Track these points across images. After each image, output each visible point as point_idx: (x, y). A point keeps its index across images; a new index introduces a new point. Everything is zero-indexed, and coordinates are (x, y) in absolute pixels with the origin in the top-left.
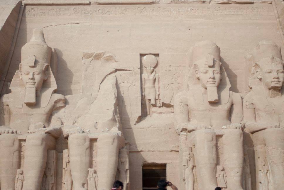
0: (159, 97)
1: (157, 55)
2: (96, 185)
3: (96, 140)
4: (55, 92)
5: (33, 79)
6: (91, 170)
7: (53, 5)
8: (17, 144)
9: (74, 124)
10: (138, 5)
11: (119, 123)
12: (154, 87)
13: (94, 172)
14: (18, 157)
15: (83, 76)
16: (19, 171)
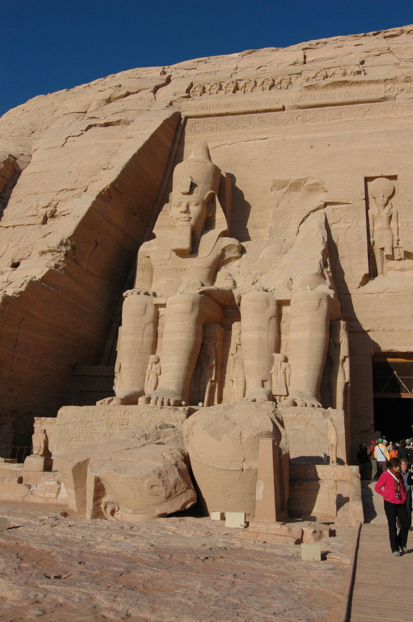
0: (398, 244)
1: (394, 178)
2: (288, 384)
3: (287, 303)
4: (224, 234)
5: (187, 211)
6: (278, 357)
7: (227, 114)
8: (151, 311)
9: (253, 284)
10: (360, 105)
11: (331, 282)
12: (390, 228)
13: (283, 359)
14: (152, 333)
15: (271, 213)
16: (152, 358)
